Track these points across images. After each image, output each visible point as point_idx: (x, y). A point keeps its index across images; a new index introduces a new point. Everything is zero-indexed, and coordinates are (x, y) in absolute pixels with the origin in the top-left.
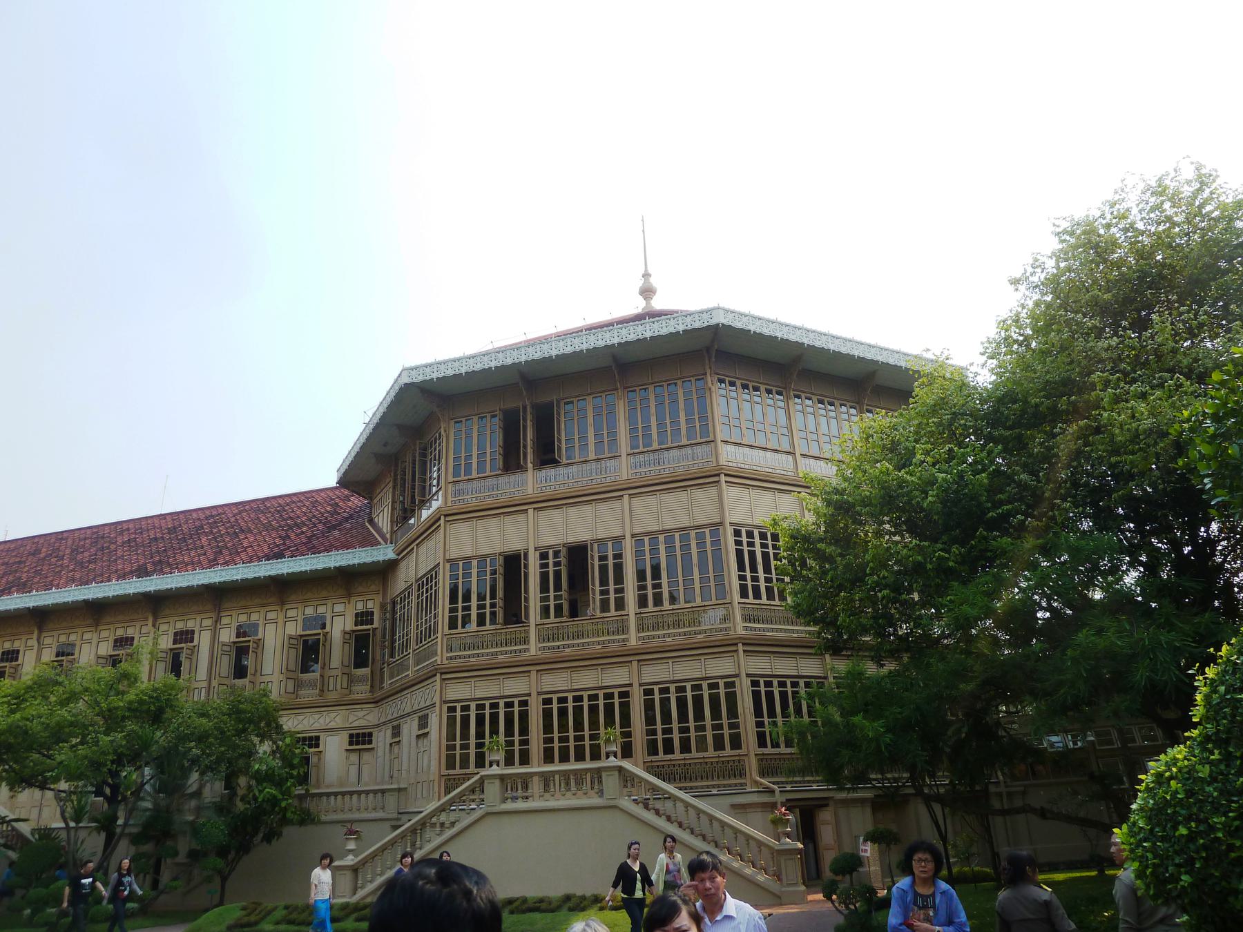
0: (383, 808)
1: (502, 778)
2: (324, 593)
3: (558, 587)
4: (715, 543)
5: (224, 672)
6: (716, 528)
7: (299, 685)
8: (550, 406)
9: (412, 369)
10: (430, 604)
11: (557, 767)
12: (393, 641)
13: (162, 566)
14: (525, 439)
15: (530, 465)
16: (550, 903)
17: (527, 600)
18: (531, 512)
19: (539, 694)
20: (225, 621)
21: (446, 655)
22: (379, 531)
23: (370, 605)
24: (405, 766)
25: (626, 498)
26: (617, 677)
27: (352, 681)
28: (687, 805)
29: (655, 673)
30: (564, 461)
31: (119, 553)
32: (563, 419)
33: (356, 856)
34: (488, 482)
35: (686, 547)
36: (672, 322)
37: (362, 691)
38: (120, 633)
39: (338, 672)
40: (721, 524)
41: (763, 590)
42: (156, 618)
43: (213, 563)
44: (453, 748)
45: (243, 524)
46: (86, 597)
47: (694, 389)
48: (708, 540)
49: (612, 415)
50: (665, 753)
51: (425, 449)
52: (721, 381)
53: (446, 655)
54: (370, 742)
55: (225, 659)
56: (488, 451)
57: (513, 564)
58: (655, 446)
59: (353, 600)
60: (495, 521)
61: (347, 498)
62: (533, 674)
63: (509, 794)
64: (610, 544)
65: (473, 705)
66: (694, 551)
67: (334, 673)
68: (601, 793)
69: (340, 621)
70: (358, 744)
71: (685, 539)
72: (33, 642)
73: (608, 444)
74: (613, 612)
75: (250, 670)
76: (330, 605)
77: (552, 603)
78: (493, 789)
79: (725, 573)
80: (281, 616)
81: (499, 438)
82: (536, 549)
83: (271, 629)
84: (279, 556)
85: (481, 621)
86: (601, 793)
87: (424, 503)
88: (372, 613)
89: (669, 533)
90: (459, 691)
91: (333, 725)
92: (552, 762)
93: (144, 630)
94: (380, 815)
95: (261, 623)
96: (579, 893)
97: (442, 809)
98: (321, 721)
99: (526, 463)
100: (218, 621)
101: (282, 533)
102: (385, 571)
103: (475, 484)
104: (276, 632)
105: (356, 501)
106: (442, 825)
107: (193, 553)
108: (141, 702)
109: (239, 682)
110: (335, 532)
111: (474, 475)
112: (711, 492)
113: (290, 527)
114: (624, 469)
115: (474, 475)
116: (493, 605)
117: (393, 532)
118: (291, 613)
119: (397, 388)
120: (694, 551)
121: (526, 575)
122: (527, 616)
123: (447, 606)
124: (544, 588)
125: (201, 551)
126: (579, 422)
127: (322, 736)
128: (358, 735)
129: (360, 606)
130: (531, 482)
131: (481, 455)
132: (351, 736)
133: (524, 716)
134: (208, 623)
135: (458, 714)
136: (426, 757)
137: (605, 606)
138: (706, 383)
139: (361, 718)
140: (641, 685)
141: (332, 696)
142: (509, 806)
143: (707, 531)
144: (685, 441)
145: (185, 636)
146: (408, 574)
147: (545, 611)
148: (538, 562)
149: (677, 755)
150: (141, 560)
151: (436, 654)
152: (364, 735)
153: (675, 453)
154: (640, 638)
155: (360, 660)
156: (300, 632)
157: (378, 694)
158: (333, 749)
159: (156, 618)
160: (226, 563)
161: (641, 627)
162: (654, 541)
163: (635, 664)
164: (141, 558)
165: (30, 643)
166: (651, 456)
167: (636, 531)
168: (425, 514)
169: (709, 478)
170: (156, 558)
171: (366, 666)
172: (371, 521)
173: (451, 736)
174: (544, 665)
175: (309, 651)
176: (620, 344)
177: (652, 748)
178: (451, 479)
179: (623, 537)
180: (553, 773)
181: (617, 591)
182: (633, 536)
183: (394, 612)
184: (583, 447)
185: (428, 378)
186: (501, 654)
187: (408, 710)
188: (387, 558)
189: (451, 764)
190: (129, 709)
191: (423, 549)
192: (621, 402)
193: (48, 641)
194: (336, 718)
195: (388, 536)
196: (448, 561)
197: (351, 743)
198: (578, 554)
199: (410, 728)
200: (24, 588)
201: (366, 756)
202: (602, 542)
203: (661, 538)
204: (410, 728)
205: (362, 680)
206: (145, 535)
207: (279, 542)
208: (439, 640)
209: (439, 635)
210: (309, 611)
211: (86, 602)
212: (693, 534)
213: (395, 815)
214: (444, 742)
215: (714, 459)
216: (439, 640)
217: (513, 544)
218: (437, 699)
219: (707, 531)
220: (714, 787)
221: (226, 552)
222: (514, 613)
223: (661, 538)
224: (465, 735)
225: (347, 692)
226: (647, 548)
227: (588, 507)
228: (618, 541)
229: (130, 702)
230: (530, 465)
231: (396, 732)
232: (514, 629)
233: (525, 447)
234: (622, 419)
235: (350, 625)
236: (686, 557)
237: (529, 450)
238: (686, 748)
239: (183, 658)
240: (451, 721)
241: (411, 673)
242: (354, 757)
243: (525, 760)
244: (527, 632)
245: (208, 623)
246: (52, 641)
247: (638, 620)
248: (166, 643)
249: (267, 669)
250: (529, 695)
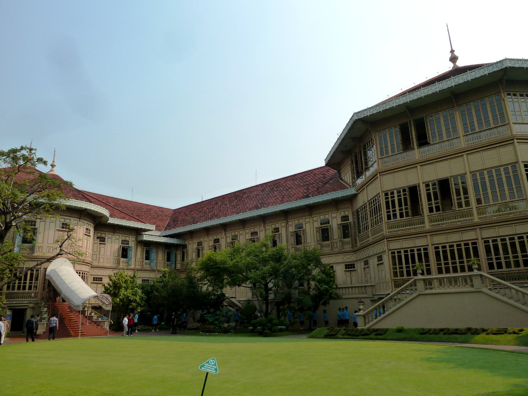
0: (366, 293)
1: (424, 280)
2: (327, 210)
3: (436, 198)
4: (515, 171)
5: (293, 243)
6: (514, 165)
7: (322, 246)
8: (422, 119)
9: (358, 113)
10: (377, 210)
11: (444, 275)
12: (359, 227)
13: (263, 205)
14: (412, 135)
15: (416, 147)
16: (461, 331)
17: (422, 205)
18: (419, 167)
19: (432, 245)
20: (290, 223)
21: (387, 231)
22: (346, 183)
23: (347, 213)
24: (372, 276)
25: (465, 156)
27: (343, 243)
28: (517, 291)
29: (489, 233)
30: (432, 143)
31: (246, 201)
32: (429, 124)
33: (364, 311)
34: (397, 156)
35: (499, 175)
36: (482, 70)
37: (348, 247)
38: (252, 230)
39: (338, 240)
40: (517, 162)
42: (264, 224)
43: (282, 202)
45: (289, 186)
46: (240, 218)
47: (495, 101)
48: (510, 171)
49: (453, 119)
50: (498, 268)
51: (365, 146)
52: (509, 95)
53: (387, 231)
54: (354, 268)
55: (292, 238)
56: (395, 143)
57: (414, 190)
58: (477, 130)
59: (339, 211)
60: (403, 172)
61: (328, 171)
62: (429, 237)
63: (428, 286)
64: (459, 177)
65: (402, 251)
66: (503, 176)
67: (336, 241)
68: (472, 286)
69: (335, 220)
70: (349, 268)
72: (223, 236)
73: (450, 131)
74: (464, 207)
75: (303, 241)
76: (330, 214)
77: (434, 206)
78: (420, 285)
79: (522, 185)
80: (311, 219)
81: (399, 137)
82: (423, 183)
83: (308, 225)
84: (307, 197)
85: (401, 216)
86: (472, 286)
87: (367, 169)
88: (348, 216)
89: (489, 170)
90: (396, 245)
91: (338, 261)
92: (450, 273)
93: (261, 229)
94: (365, 296)
95: (304, 223)
96: (474, 327)
97: (398, 293)
98: (333, 260)
99: (413, 145)
100: (287, 223)
101: (306, 187)
102: (351, 199)
103: (391, 158)
104: (311, 226)
105: (333, 172)
106: (399, 299)
107: (273, 198)
108: (274, 255)
109: (299, 246)
110: (327, 185)
111: (390, 154)
112: (510, 148)
113: (308, 185)
114: (462, 143)
115: (390, 154)
116: (406, 209)
117: (353, 183)
118: (315, 219)
119: (352, 122)
120: (503, 176)
121: (420, 194)
122: (423, 212)
123: (385, 211)
124: (429, 199)
125: (276, 198)
126: (437, 124)
127: (334, 265)
128: (349, 265)
129: (343, 214)
130: (417, 154)
131: (392, 145)
132: (346, 265)
134: (283, 224)
135: (396, 254)
136: (383, 273)
137: (460, 205)
138: (501, 96)
139: (350, 258)
140: (482, 239)
141: (336, 250)
142: (429, 291)
143: (510, 167)
144: (492, 126)
145: (277, 230)
146: (362, 200)
147: (431, 210)
148: (425, 189)
149: (504, 269)
150: (255, 204)
151: (383, 231)
152: (351, 265)
154: (479, 218)
155: (345, 235)
156: (320, 226)
157: (355, 248)
158: (340, 272)
159: (264, 224)
160: (287, 201)
161: (479, 214)
162: (482, 174)
163: (478, 230)
164: (255, 202)
165: (222, 236)
167: (472, 170)
168: (368, 174)
169: (509, 141)
170: (260, 202)
171: (349, 237)
172: (341, 179)
173: (394, 264)
174: (433, 232)
175: (325, 233)
176: (455, 86)
177: (491, 266)
178: (380, 157)
179: (466, 174)
180: (443, 278)
181: (465, 198)
182: (470, 172)
183: (358, 215)
184: (441, 135)
185: (366, 115)
186: (412, 229)
187: (371, 254)
188: (352, 193)
190: (270, 257)
191: (369, 188)
192: (457, 113)
193: (228, 235)
194: (339, 258)
195: (351, 184)
196: (383, 192)
197: (346, 268)
198: (444, 184)
199: (373, 262)
200: (217, 216)
201: (353, 273)
202: (455, 177)
203: (485, 172)
204: (373, 262)
205: (347, 243)
206: (253, 193)
207: (306, 191)
208: (384, 224)
209: (384, 222)
210: (322, 217)
212: (502, 169)
213: (371, 296)
214: (392, 267)
215: (509, 132)
216: (384, 224)
217: (412, 182)
218: (386, 248)
219: (510, 167)
220: (525, 283)
221: (285, 197)
222: (416, 210)
223: (485, 172)
224: (400, 263)
225: (342, 248)
226: (478, 177)
228: (463, 176)
229: (270, 255)
230: (416, 147)
231: (366, 263)
232: (416, 218)
233: (412, 139)
234: (458, 120)
235: (339, 222)
236: (500, 180)
237: (415, 140)
238: (508, 265)
239: (277, 239)
240: (393, 258)
241: (371, 239)
242: (348, 273)
243: (429, 272)
244: (424, 219)
245: (283, 224)
246: (230, 235)
247: (477, 210)
248: (269, 233)
249: (309, 240)
250: (428, 245)
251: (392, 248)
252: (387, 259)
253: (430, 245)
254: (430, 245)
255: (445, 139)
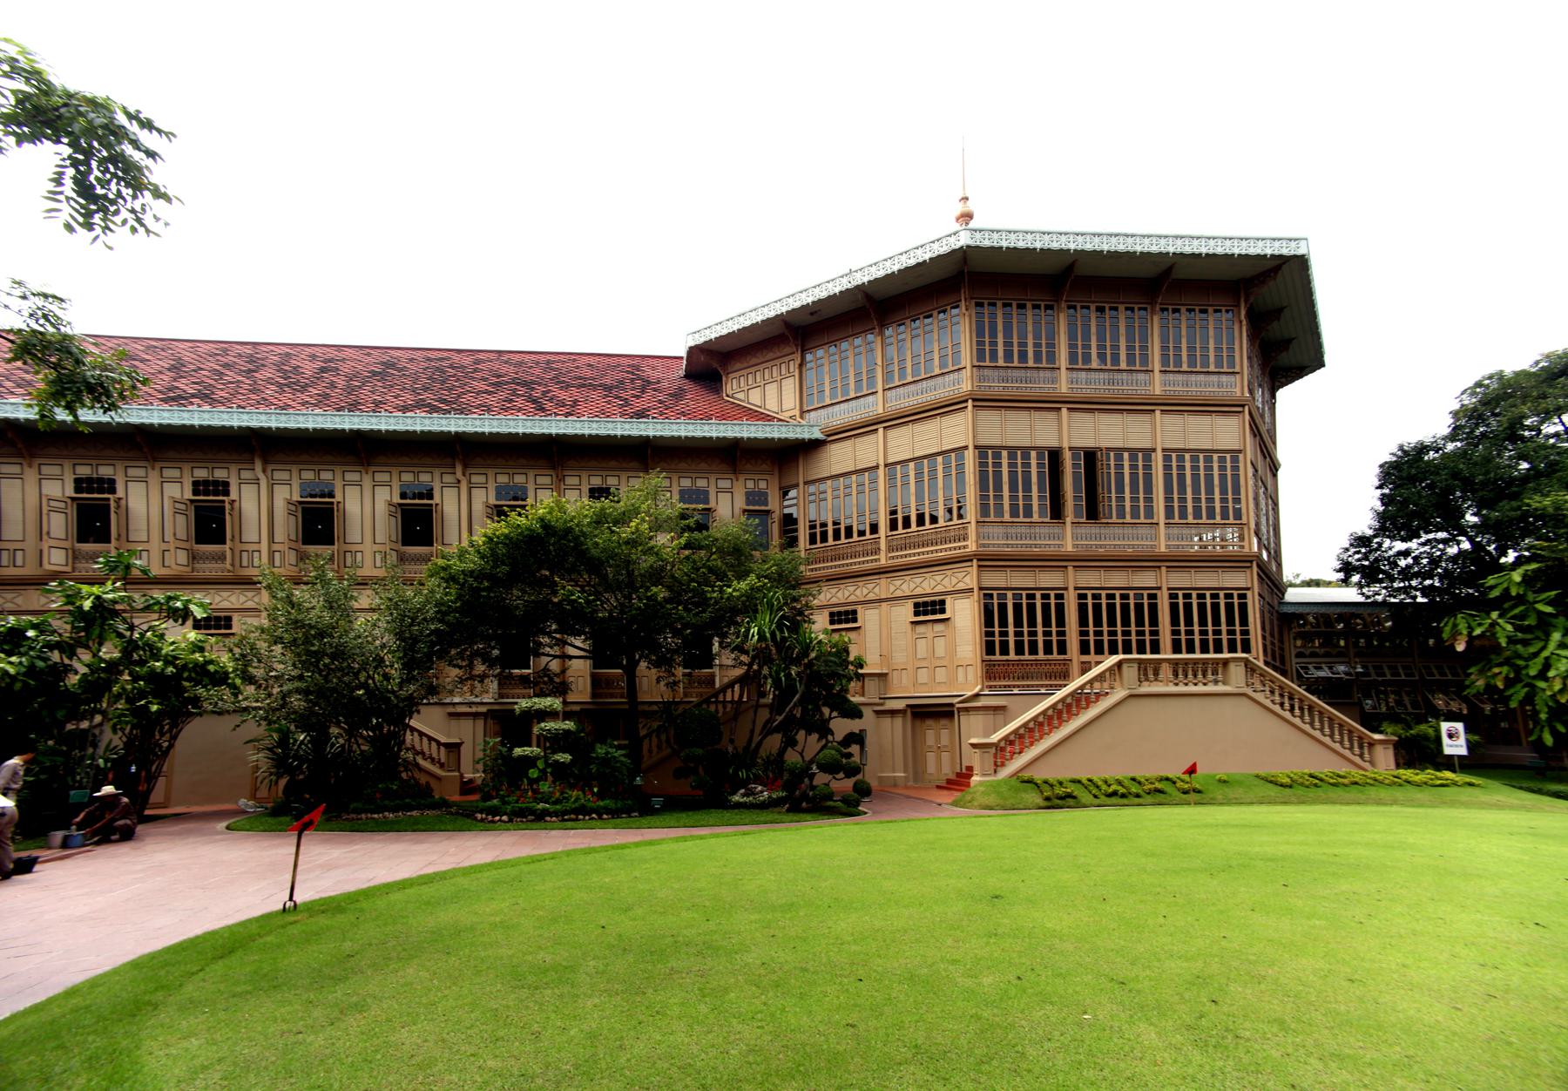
18: (1064, 411)
26: (1146, 579)
41: (1218, 510)
44: (991, 634)
71: (1208, 460)
120: (1216, 472)
133: (1060, 609)
153: (1202, 377)
154: (1168, 546)
166: (1180, 377)
173: (988, 622)
179: (1154, 450)
189: (989, 648)
211: (358, 435)
227: (1119, 416)
228: (1148, 453)
251: (986, 584)
252: (965, 615)
253: (1071, 589)
254: (1071, 589)
255: (1123, 365)
